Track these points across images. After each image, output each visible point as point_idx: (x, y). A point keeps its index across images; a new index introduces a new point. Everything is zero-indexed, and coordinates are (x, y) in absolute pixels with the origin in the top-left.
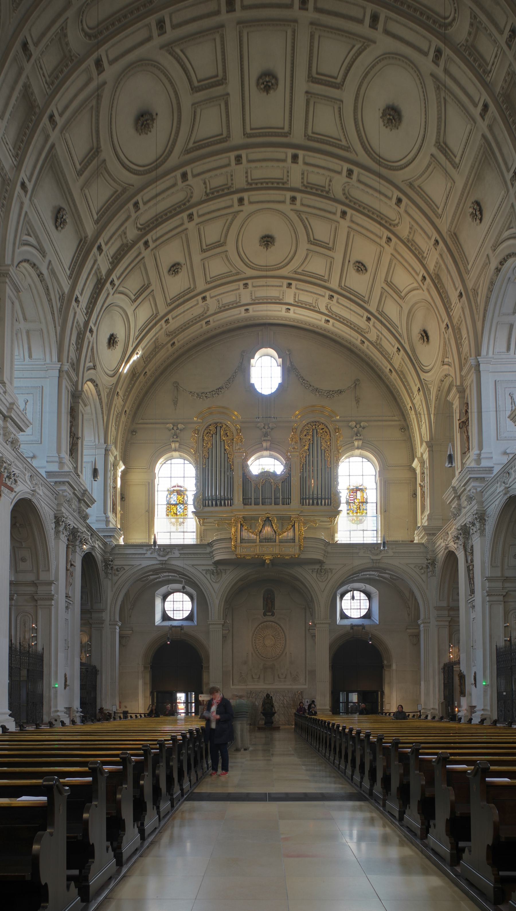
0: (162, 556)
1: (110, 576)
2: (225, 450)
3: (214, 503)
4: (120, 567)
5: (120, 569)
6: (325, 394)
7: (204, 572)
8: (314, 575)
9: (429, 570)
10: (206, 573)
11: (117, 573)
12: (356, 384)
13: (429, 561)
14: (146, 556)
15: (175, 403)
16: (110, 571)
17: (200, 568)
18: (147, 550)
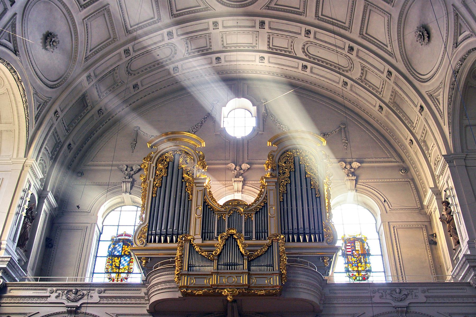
0: (73, 301)
2: (183, 178)
14: (49, 300)
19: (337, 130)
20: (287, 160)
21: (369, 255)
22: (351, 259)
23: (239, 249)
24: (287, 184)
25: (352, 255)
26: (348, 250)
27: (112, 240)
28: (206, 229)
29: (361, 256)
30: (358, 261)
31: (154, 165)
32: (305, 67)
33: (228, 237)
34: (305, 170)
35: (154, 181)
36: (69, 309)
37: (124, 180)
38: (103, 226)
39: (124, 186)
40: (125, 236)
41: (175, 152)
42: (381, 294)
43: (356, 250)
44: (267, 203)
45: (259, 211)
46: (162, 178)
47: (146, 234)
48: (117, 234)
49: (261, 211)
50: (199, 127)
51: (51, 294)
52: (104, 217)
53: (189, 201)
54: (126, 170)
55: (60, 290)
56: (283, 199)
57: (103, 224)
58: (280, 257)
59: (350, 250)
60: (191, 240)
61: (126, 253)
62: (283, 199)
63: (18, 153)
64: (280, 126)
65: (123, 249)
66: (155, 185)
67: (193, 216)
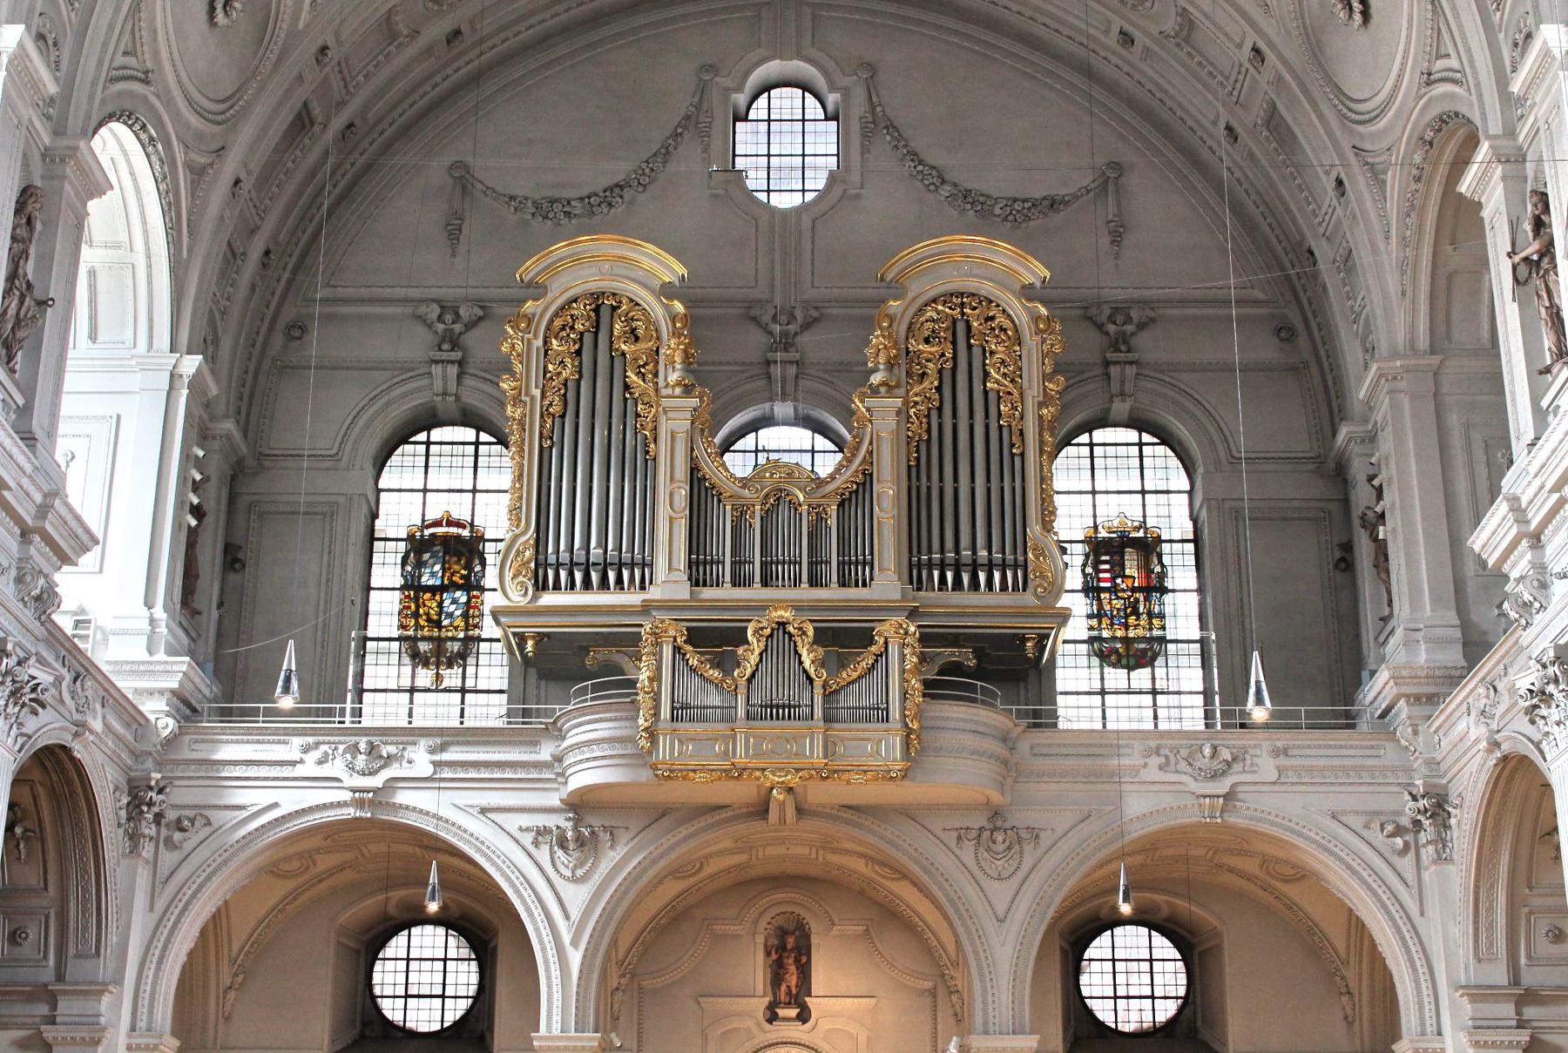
1: (147, 850)
2: (627, 387)
3: (578, 576)
4: (191, 813)
6: (997, 211)
7: (527, 839)
8: (967, 853)
9: (1423, 837)
10: (536, 843)
11: (177, 836)
12: (1110, 180)
13: (1423, 803)
14: (299, 771)
15: (454, 232)
16: (149, 830)
17: (513, 822)
18: (306, 749)
20: (933, 331)
21: (1164, 590)
22: (1110, 603)
23: (801, 663)
24: (929, 409)
25: (1114, 590)
26: (1101, 575)
27: (410, 538)
28: (701, 551)
31: (539, 342)
33: (773, 629)
36: (357, 795)
37: (438, 355)
38: (379, 491)
41: (598, 298)
42: (1163, 760)
43: (1124, 576)
44: (871, 475)
45: (850, 499)
46: (565, 385)
47: (533, 565)
48: (423, 521)
49: (854, 496)
51: (304, 756)
53: (646, 460)
54: (440, 318)
55: (324, 743)
56: (918, 459)
58: (903, 680)
59: (1107, 575)
62: (918, 459)
63: (151, 337)
67: (663, 511)
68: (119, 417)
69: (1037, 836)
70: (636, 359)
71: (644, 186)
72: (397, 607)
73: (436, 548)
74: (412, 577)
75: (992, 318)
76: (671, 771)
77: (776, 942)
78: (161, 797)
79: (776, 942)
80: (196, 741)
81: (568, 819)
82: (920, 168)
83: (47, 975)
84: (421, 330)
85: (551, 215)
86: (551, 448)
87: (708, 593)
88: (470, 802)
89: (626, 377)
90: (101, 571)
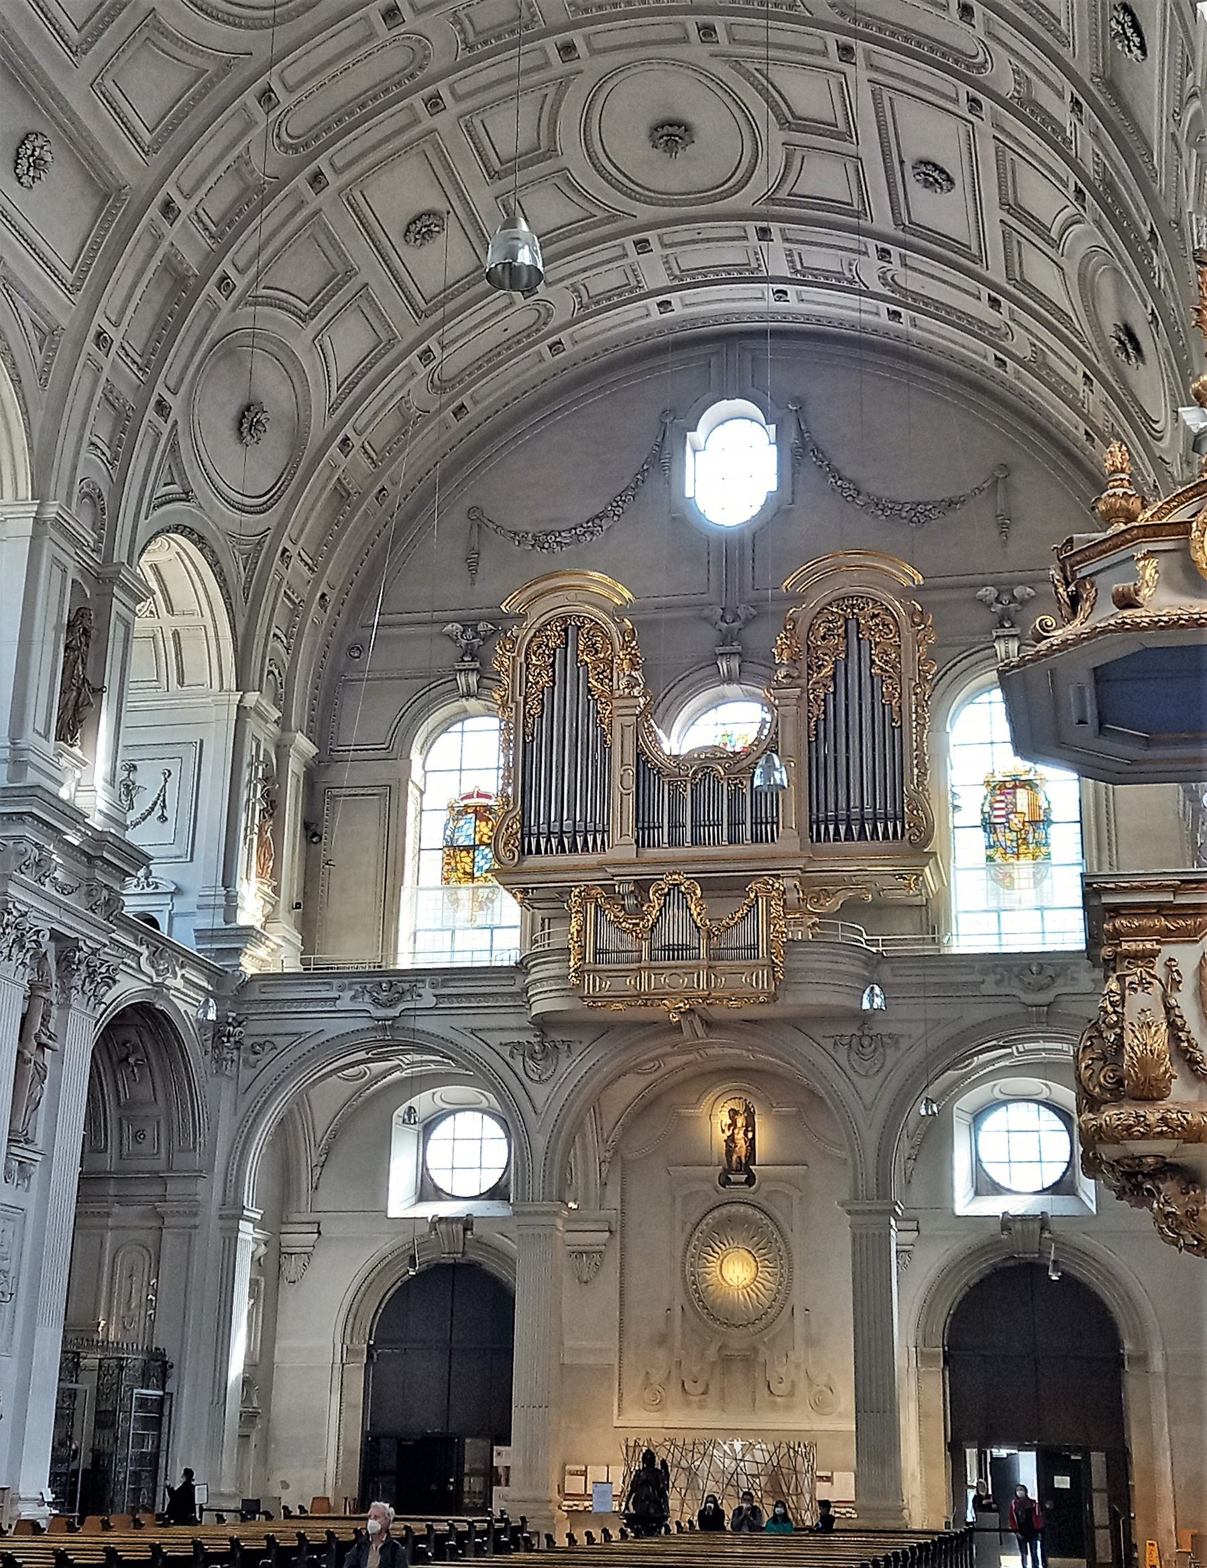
0: (384, 1006)
1: (230, 1070)
2: (590, 690)
4: (261, 1040)
5: (262, 1045)
6: (904, 514)
8: (842, 1055)
11: (253, 1058)
14: (340, 1005)
15: (472, 563)
17: (495, 1039)
18: (342, 988)
19: (984, 485)
21: (1048, 822)
23: (691, 915)
24: (825, 694)
29: (1027, 828)
30: (1020, 841)
32: (895, 315)
33: (669, 889)
34: (871, 654)
35: (526, 703)
39: (461, 680)
40: (478, 797)
42: (999, 977)
43: (1016, 813)
46: (543, 692)
47: (519, 835)
50: (629, 500)
52: (425, 752)
55: (356, 983)
57: (424, 767)
60: (597, 898)
61: (485, 839)
62: (817, 735)
64: (836, 483)
65: (477, 829)
66: (529, 712)
68: (202, 741)
69: (897, 1042)
70: (596, 669)
71: (619, 516)
72: (440, 864)
73: (469, 816)
74: (451, 839)
75: (874, 616)
76: (594, 1002)
77: (730, 1122)
78: (239, 1029)
79: (730, 1122)
80: (265, 986)
81: (536, 1036)
82: (839, 483)
83: (160, 1164)
84: (450, 643)
85: (546, 545)
86: (532, 741)
87: (650, 853)
88: (468, 1025)
89: (589, 682)
90: (191, 860)
